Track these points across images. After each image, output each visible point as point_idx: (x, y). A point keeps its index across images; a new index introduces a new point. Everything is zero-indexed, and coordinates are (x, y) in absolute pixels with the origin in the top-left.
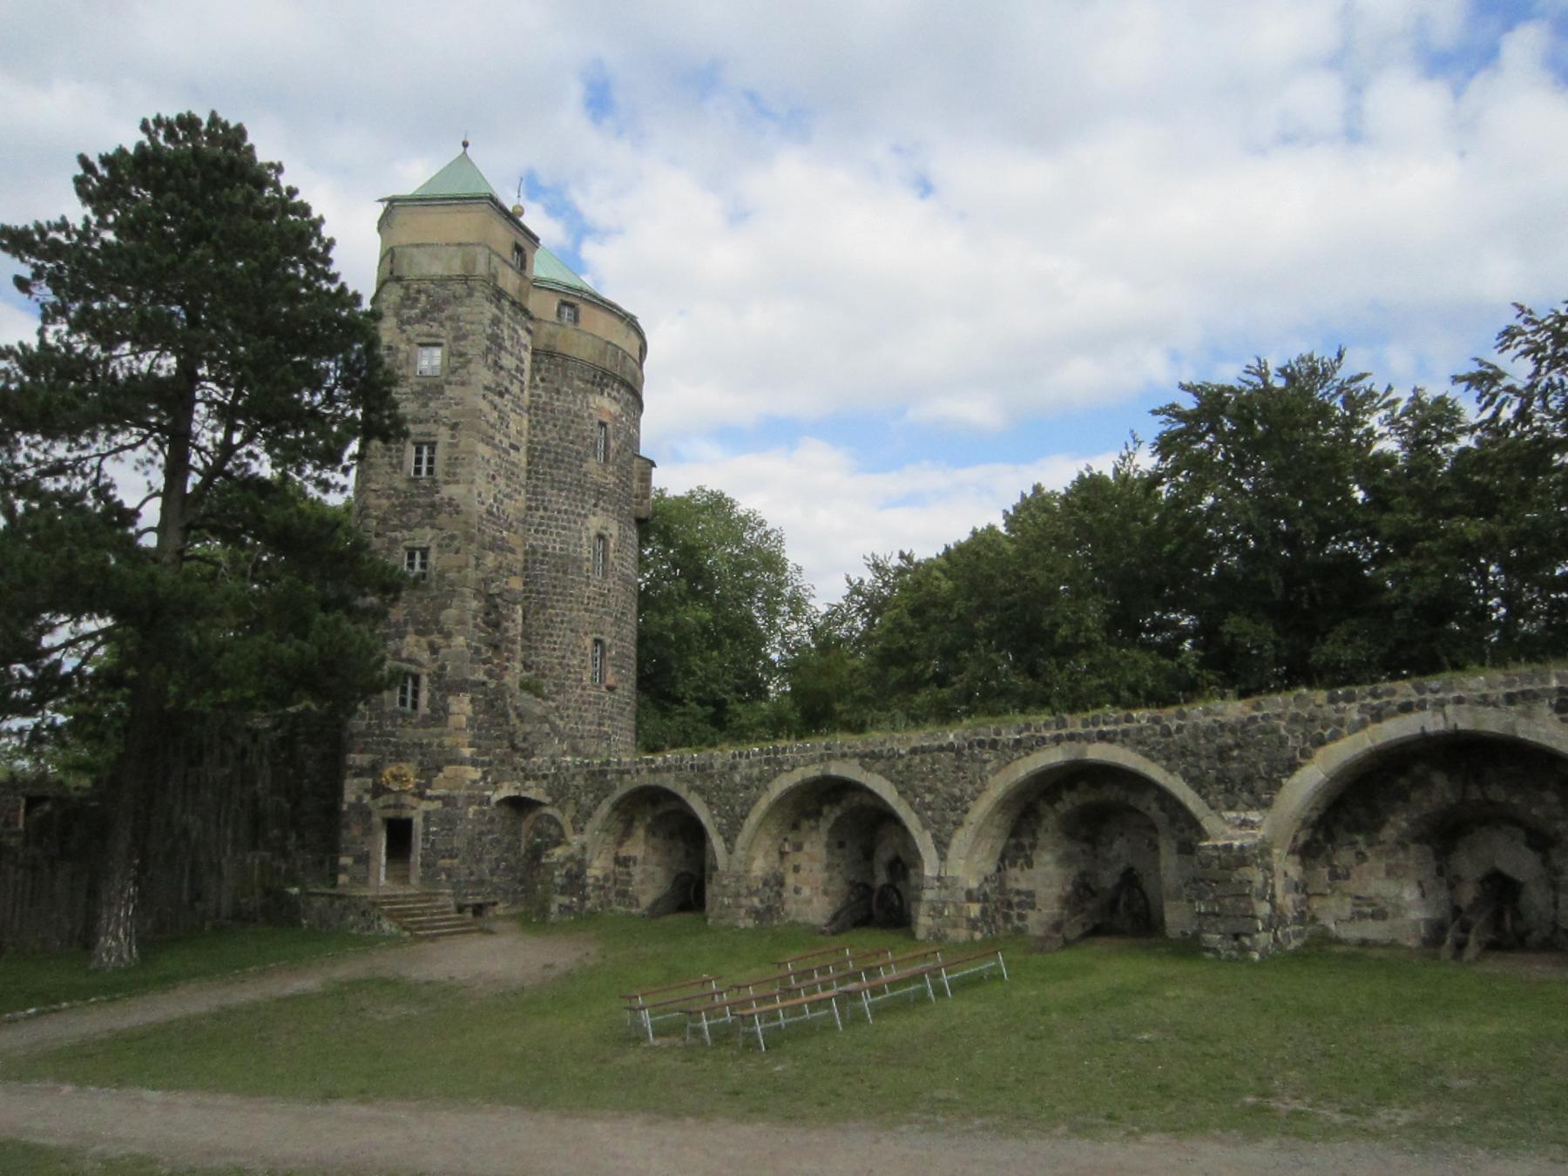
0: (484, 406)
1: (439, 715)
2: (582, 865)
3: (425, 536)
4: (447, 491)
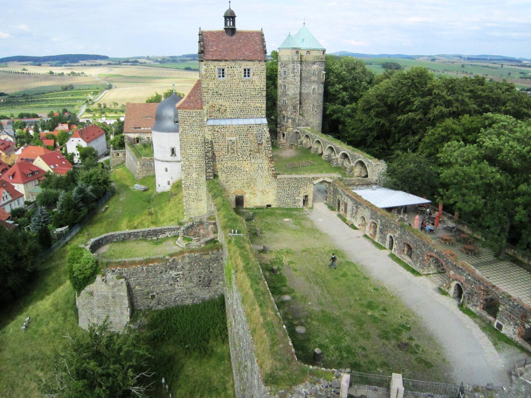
0: (292, 80)
1: (287, 122)
2: (302, 142)
3: (285, 99)
4: (287, 93)
